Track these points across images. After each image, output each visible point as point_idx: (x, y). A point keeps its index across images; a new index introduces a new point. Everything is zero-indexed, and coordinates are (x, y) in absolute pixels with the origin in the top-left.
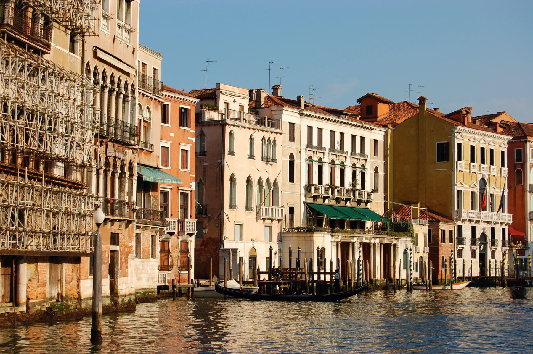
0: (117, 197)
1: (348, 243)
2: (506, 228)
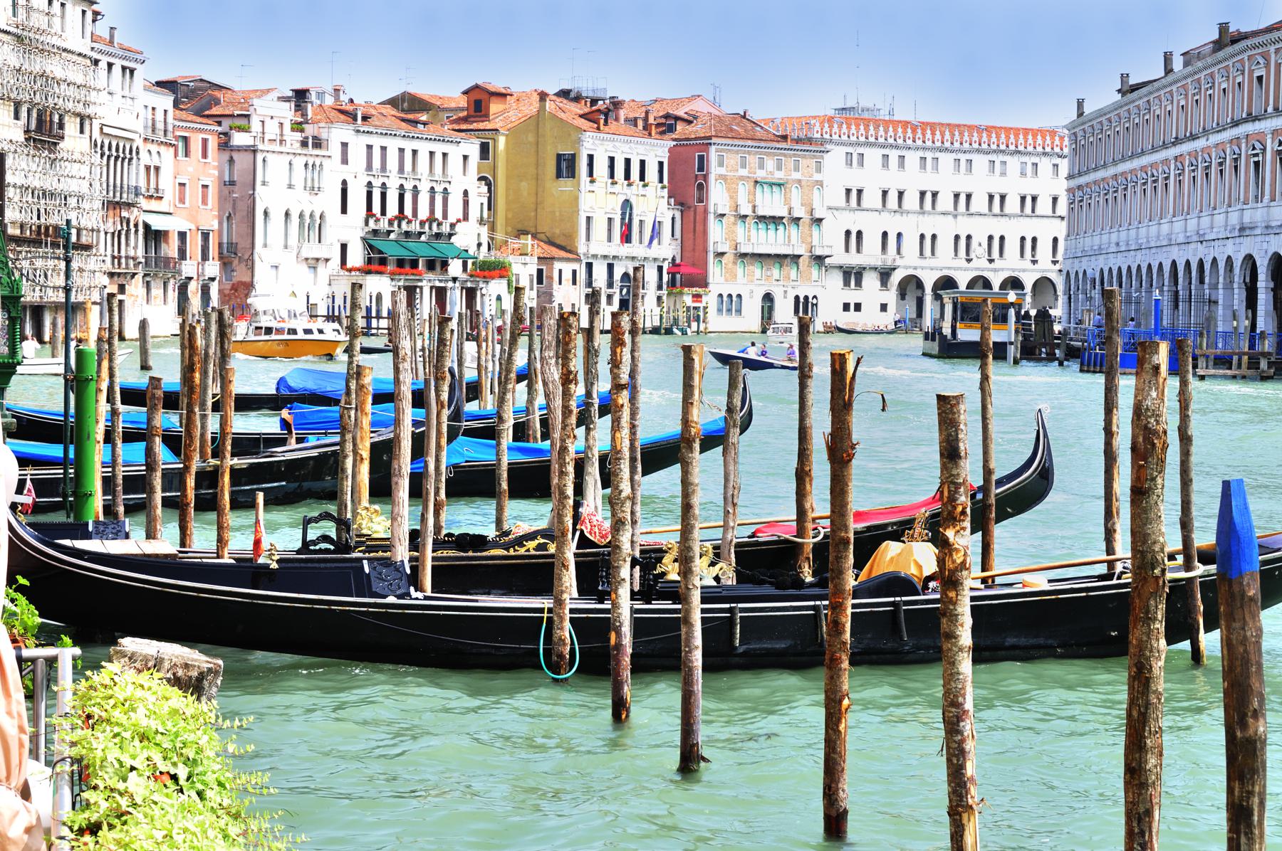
0: (123, 253)
2: (666, 266)
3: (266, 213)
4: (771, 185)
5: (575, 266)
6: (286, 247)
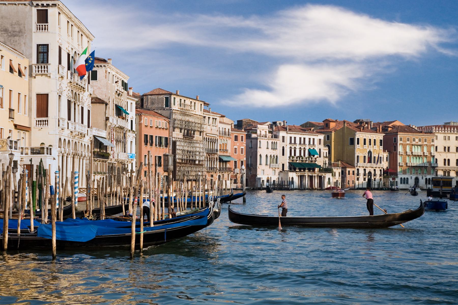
1: (303, 176)
3: (260, 156)
4: (417, 145)
5: (353, 170)
6: (266, 165)
